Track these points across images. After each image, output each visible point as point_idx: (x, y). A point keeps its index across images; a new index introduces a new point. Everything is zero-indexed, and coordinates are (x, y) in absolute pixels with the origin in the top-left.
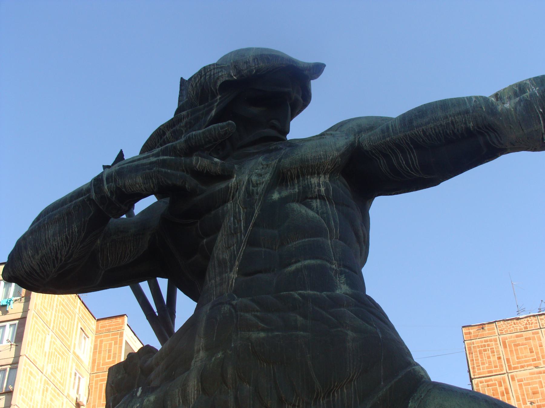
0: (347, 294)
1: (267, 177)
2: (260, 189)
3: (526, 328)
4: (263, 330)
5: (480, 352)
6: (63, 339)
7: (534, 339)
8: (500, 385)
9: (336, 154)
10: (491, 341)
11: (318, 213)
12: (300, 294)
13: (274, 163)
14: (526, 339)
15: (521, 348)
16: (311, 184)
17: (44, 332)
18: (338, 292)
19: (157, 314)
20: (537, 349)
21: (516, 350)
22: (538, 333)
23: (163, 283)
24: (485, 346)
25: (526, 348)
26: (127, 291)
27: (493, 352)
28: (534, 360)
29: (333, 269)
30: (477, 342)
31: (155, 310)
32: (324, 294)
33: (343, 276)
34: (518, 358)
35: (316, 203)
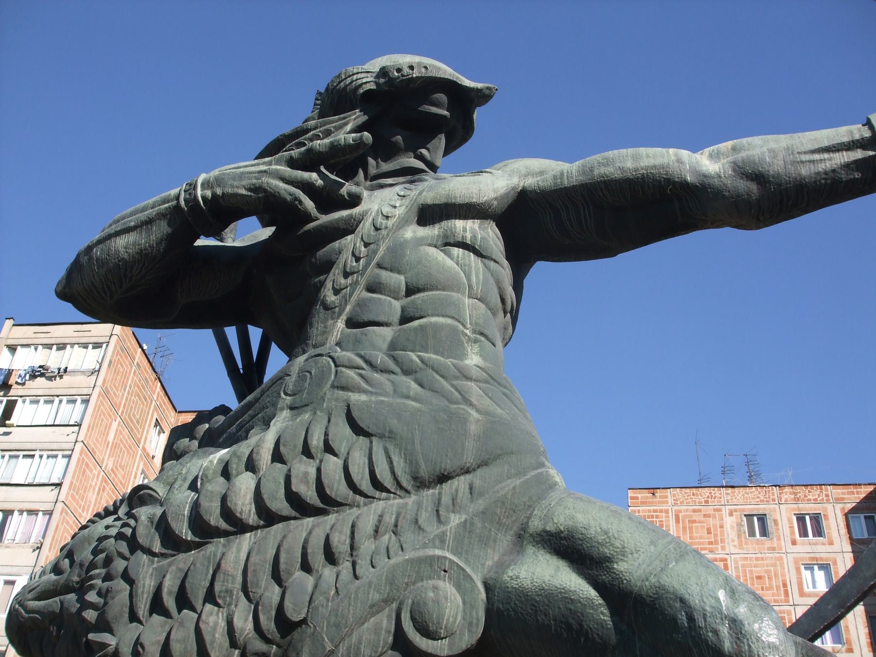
0: (478, 367)
3: (707, 502)
4: (365, 392)
6: (132, 430)
7: (714, 517)
9: (492, 195)
10: (661, 511)
11: (457, 264)
12: (419, 357)
13: (413, 194)
15: (697, 527)
16: (455, 228)
17: (110, 417)
18: (467, 362)
19: (242, 371)
20: (716, 530)
21: (691, 528)
22: (720, 510)
23: (255, 334)
24: (652, 517)
25: (703, 527)
26: (206, 336)
28: (710, 543)
29: (466, 335)
30: (644, 511)
31: (240, 366)
32: (449, 361)
33: (477, 346)
34: (691, 538)
35: (457, 251)
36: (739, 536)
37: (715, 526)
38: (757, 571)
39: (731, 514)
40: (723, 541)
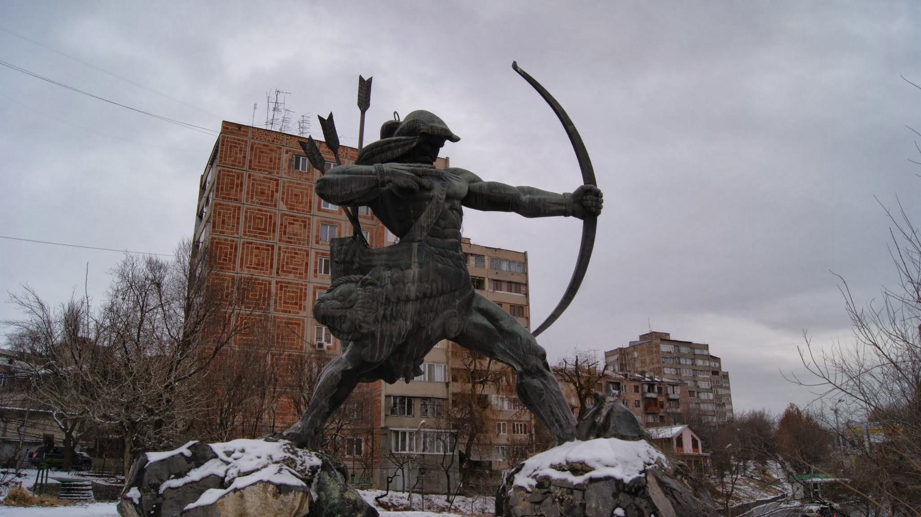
1: (444, 197)
2: (442, 201)
5: (231, 147)
14: (270, 150)
27: (241, 150)
36: (289, 167)
37: (275, 158)
38: (297, 191)
39: (287, 153)
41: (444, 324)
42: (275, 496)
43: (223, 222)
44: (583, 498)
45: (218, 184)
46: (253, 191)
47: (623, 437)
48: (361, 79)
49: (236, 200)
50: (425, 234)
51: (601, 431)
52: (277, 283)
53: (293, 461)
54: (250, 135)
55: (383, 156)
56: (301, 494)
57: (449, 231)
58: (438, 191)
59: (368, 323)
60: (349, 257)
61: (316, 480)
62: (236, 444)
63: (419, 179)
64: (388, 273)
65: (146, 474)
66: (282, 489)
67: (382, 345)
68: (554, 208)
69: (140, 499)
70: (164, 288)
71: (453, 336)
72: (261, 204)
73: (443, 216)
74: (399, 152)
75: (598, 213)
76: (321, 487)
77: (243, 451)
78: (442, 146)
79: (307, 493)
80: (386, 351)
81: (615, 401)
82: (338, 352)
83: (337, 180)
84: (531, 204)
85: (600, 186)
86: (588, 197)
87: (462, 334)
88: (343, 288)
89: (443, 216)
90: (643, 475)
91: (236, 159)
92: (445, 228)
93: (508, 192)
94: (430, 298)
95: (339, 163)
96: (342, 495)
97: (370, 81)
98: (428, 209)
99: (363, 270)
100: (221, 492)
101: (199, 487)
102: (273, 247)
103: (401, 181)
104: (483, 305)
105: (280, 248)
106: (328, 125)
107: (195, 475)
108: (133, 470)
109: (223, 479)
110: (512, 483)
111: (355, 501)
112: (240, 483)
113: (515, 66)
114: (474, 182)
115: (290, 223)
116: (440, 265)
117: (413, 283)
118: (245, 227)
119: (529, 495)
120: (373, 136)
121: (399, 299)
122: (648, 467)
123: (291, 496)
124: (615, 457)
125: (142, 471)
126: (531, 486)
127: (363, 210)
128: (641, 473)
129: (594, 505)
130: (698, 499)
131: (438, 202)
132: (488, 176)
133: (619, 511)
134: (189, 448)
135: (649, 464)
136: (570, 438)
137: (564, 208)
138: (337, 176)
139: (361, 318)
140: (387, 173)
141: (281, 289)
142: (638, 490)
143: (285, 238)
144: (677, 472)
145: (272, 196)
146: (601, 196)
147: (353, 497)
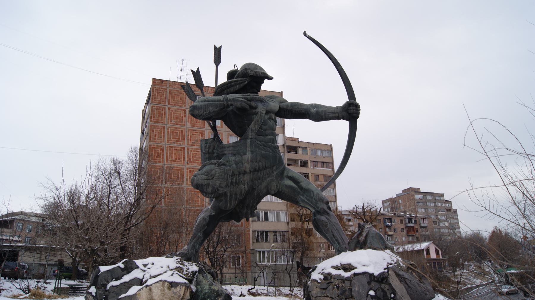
1: (265, 112)
2: (263, 115)
5: (158, 93)
8: (163, 110)
21: (174, 97)
27: (163, 94)
28: (181, 103)
35: (271, 120)
40: (185, 103)
41: (267, 186)
42: (169, 289)
43: (155, 136)
44: (351, 285)
45: (152, 114)
46: (171, 117)
47: (375, 249)
48: (215, 47)
49: (162, 123)
50: (254, 134)
51: (362, 245)
52: (187, 169)
53: (182, 269)
54: (168, 85)
55: (228, 90)
56: (184, 287)
57: (268, 132)
58: (261, 109)
59: (222, 187)
60: (210, 151)
61: (195, 279)
62: (149, 260)
63: (249, 102)
64: (233, 158)
65: (99, 279)
66: (173, 285)
67: (231, 200)
68: (332, 115)
69: (96, 293)
70: (121, 175)
71: (273, 193)
72: (176, 124)
73: (264, 123)
74: (237, 87)
75: (358, 117)
76: (198, 284)
77: (153, 264)
78: (263, 83)
79: (187, 287)
80: (234, 203)
81: (370, 227)
82: (206, 205)
83: (201, 106)
84: (318, 114)
85: (358, 101)
86: (351, 108)
87: (279, 191)
88: (208, 168)
89: (264, 123)
90: (386, 270)
91: (161, 99)
92: (266, 130)
93: (304, 107)
94: (258, 171)
95: (204, 96)
96: (210, 288)
97: (220, 48)
98: (255, 120)
99: (219, 157)
100: (140, 287)
101: (128, 285)
102: (184, 148)
103: (238, 104)
104: (290, 174)
105: (188, 149)
106: (197, 75)
107: (127, 278)
108: (92, 276)
109: (142, 280)
110: (310, 278)
111: (218, 291)
112: (149, 282)
113: (305, 34)
114: (282, 102)
115: (193, 134)
116: (263, 152)
117: (248, 163)
118: (168, 138)
119: (319, 284)
120: (223, 79)
121: (240, 173)
122: (390, 266)
123: (178, 288)
124: (370, 261)
125: (97, 277)
126: (320, 279)
127: (219, 123)
128: (385, 269)
129: (357, 289)
130: (422, 284)
131: (261, 116)
132: (290, 97)
133: (372, 293)
134: (122, 263)
135: (391, 264)
136: (345, 251)
137: (337, 115)
138: (201, 103)
139: (218, 185)
140: (230, 100)
141: (190, 172)
142: (383, 279)
143: (191, 143)
144: (409, 268)
145: (182, 119)
146: (359, 106)
147: (216, 289)
